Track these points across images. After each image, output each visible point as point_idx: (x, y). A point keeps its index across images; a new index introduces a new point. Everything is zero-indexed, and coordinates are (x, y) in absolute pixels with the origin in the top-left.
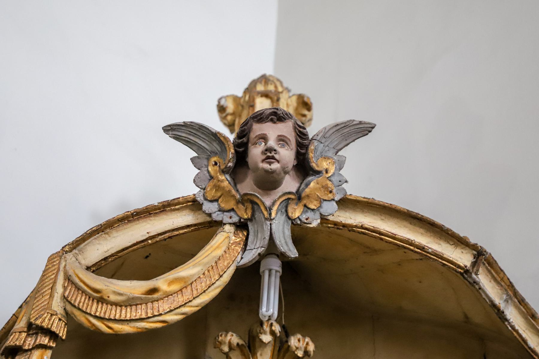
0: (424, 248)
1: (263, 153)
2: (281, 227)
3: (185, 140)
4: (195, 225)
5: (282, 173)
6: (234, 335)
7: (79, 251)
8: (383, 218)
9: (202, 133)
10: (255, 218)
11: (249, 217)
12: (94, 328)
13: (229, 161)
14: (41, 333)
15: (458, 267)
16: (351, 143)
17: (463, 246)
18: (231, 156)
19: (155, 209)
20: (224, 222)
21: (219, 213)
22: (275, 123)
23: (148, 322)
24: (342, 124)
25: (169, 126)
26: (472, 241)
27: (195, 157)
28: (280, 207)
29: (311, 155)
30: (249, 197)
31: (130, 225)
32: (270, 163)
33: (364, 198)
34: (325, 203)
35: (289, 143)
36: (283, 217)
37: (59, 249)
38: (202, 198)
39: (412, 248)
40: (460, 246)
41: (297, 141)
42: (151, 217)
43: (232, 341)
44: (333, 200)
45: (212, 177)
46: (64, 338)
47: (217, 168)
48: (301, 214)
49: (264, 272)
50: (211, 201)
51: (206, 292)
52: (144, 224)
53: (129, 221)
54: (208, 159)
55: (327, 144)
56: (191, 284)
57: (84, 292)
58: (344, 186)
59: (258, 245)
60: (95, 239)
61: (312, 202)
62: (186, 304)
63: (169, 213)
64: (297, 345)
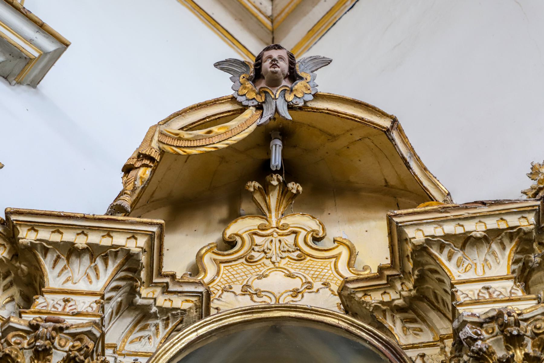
0: (363, 119)
1: (271, 63)
2: (282, 105)
3: (226, 69)
4: (233, 111)
5: (281, 74)
6: (257, 182)
7: (168, 125)
8: (339, 105)
9: (236, 64)
10: (267, 101)
11: (264, 101)
12: (176, 153)
13: (251, 73)
14: (145, 159)
15: (383, 128)
16: (319, 69)
17: (385, 117)
18: (252, 70)
19: (210, 103)
20: (249, 105)
21: (246, 101)
22: (276, 49)
23: (206, 148)
24: (314, 57)
25: (218, 63)
26: (390, 113)
27: (232, 77)
28: (281, 94)
29: (297, 68)
30: (263, 89)
31: (196, 111)
32: (274, 68)
33: (328, 93)
34: (306, 95)
35: (284, 60)
36: (283, 100)
37: (157, 123)
38: (237, 95)
39: (356, 119)
40: (383, 117)
41: (289, 60)
42: (208, 107)
43: (255, 185)
44: (310, 94)
45: (242, 84)
46: (158, 160)
47: (245, 79)
48: (293, 100)
49: (272, 147)
50: (242, 96)
51: (240, 134)
52: (204, 111)
53: (195, 109)
54: (239, 77)
55: (306, 66)
56: (231, 130)
57: (170, 137)
58: (316, 88)
59: (269, 114)
60: (177, 119)
61: (299, 94)
62: (228, 138)
63: (218, 105)
64: (292, 186)
